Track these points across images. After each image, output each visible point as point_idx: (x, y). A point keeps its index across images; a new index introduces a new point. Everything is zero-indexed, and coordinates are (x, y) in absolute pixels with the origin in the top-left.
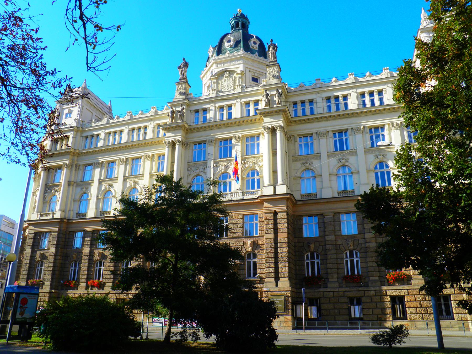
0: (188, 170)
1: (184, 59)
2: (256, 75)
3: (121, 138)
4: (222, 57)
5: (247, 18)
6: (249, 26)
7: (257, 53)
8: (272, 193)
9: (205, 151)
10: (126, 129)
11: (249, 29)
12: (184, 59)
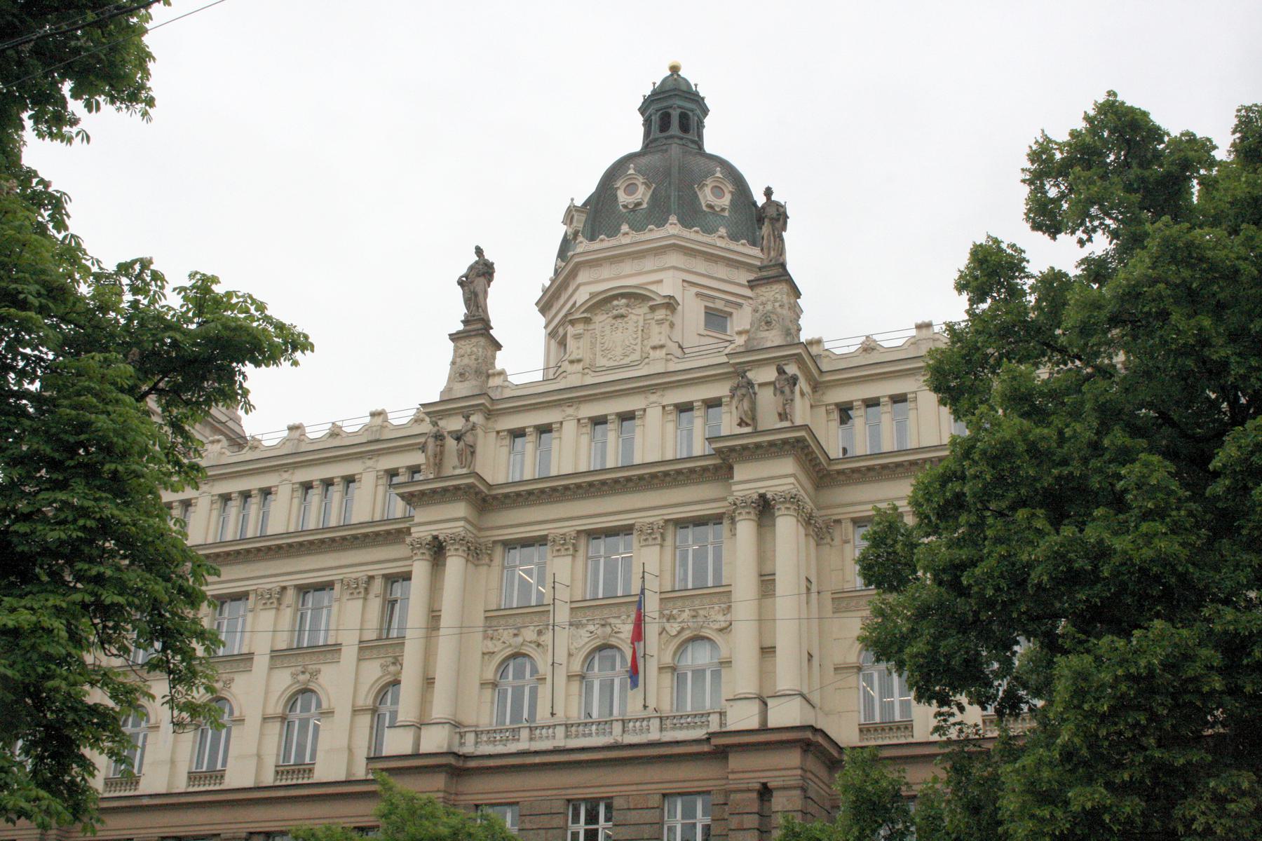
0: (485, 637)
1: (479, 251)
2: (719, 305)
3: (265, 517)
4: (606, 244)
5: (697, 94)
6: (707, 121)
7: (722, 231)
8: (754, 724)
10: (284, 485)
11: (705, 131)
12: (479, 251)
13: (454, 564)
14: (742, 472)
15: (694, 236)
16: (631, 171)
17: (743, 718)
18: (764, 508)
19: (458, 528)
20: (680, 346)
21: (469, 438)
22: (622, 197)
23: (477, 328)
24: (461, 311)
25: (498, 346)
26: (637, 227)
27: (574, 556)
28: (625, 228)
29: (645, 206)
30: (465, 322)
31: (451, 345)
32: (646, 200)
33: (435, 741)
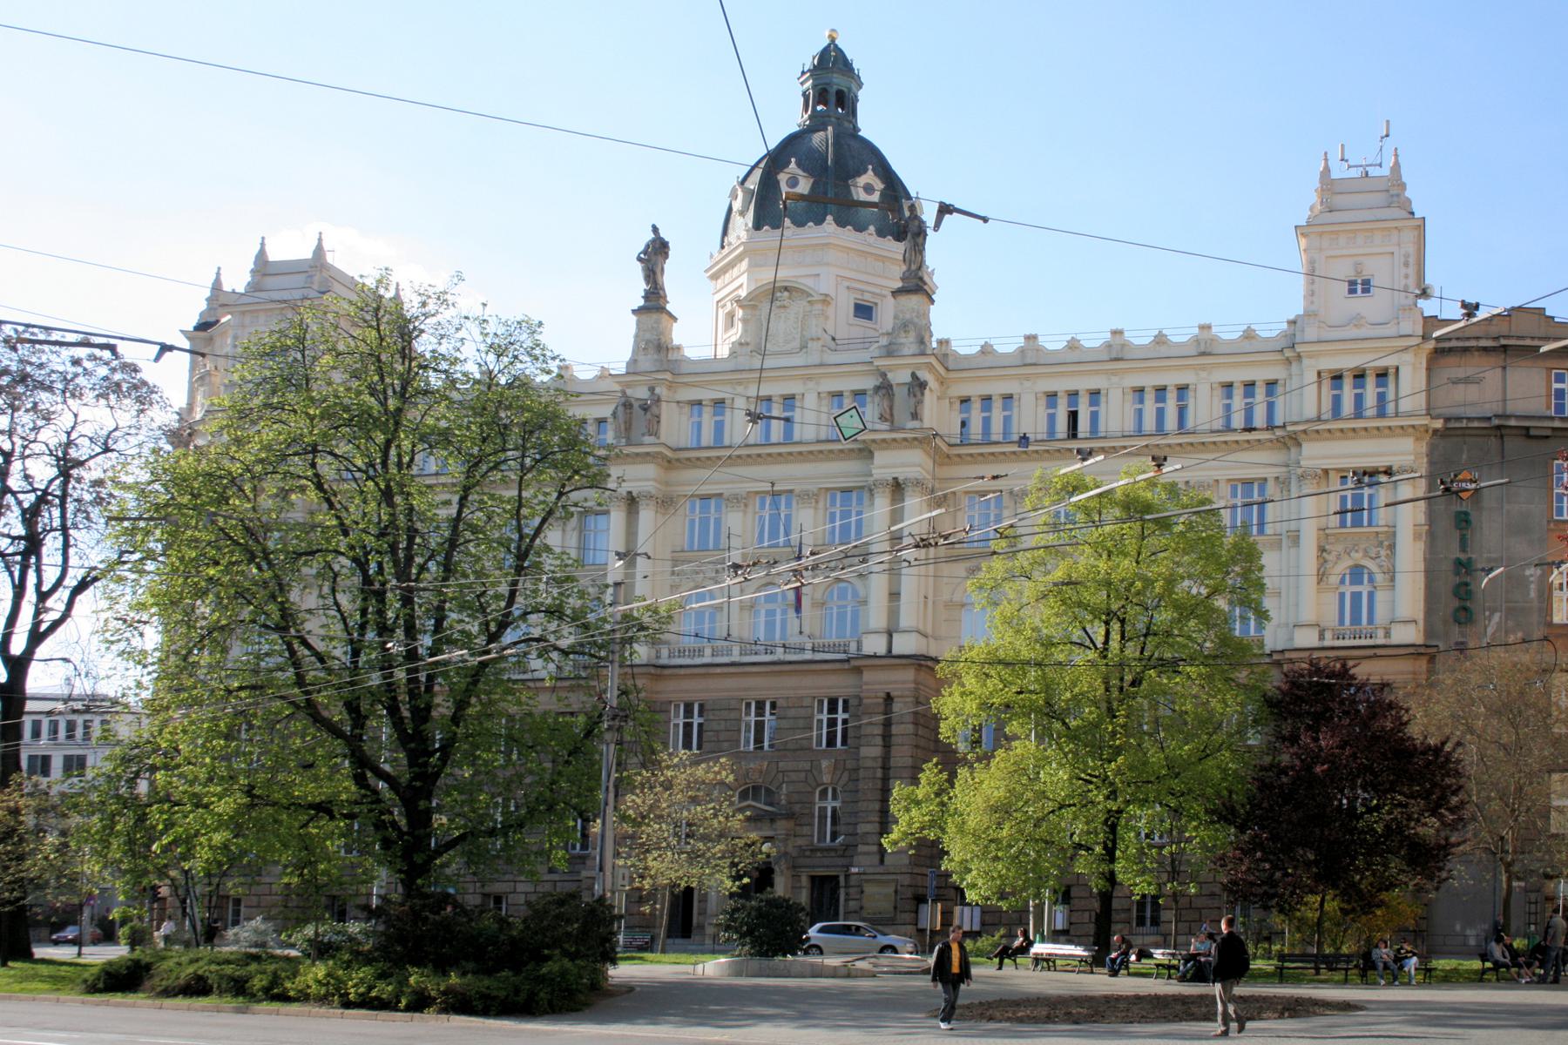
1: (655, 229)
2: (867, 297)
6: (861, 94)
7: (872, 229)
8: (882, 651)
9: (718, 522)
11: (859, 106)
12: (655, 229)
13: (646, 516)
14: (880, 457)
16: (793, 165)
17: (875, 645)
18: (898, 488)
19: (650, 486)
21: (654, 410)
23: (654, 302)
24: (641, 286)
25: (675, 319)
26: (799, 223)
27: (745, 512)
30: (646, 297)
31: (634, 318)
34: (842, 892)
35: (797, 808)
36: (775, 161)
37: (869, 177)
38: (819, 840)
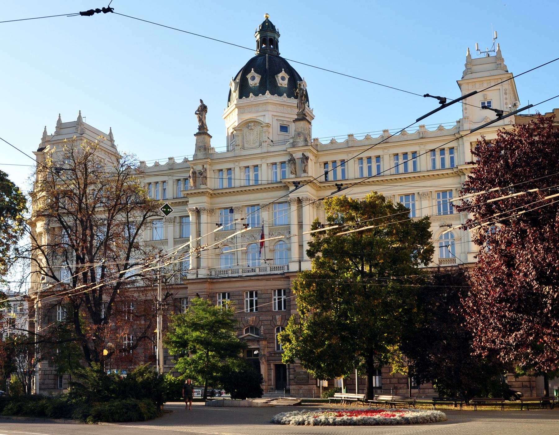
1: (201, 101)
2: (285, 123)
6: (279, 39)
7: (285, 95)
11: (280, 44)
12: (201, 101)
13: (204, 217)
15: (276, 98)
16: (252, 71)
20: (272, 141)
21: (204, 174)
22: (251, 82)
23: (203, 131)
24: (197, 124)
25: (211, 137)
26: (256, 95)
28: (251, 94)
29: (258, 85)
30: (199, 129)
31: (195, 138)
32: (258, 82)
33: (203, 273)
34: (287, 370)
35: (268, 336)
36: (245, 70)
37: (283, 74)
38: (277, 349)
